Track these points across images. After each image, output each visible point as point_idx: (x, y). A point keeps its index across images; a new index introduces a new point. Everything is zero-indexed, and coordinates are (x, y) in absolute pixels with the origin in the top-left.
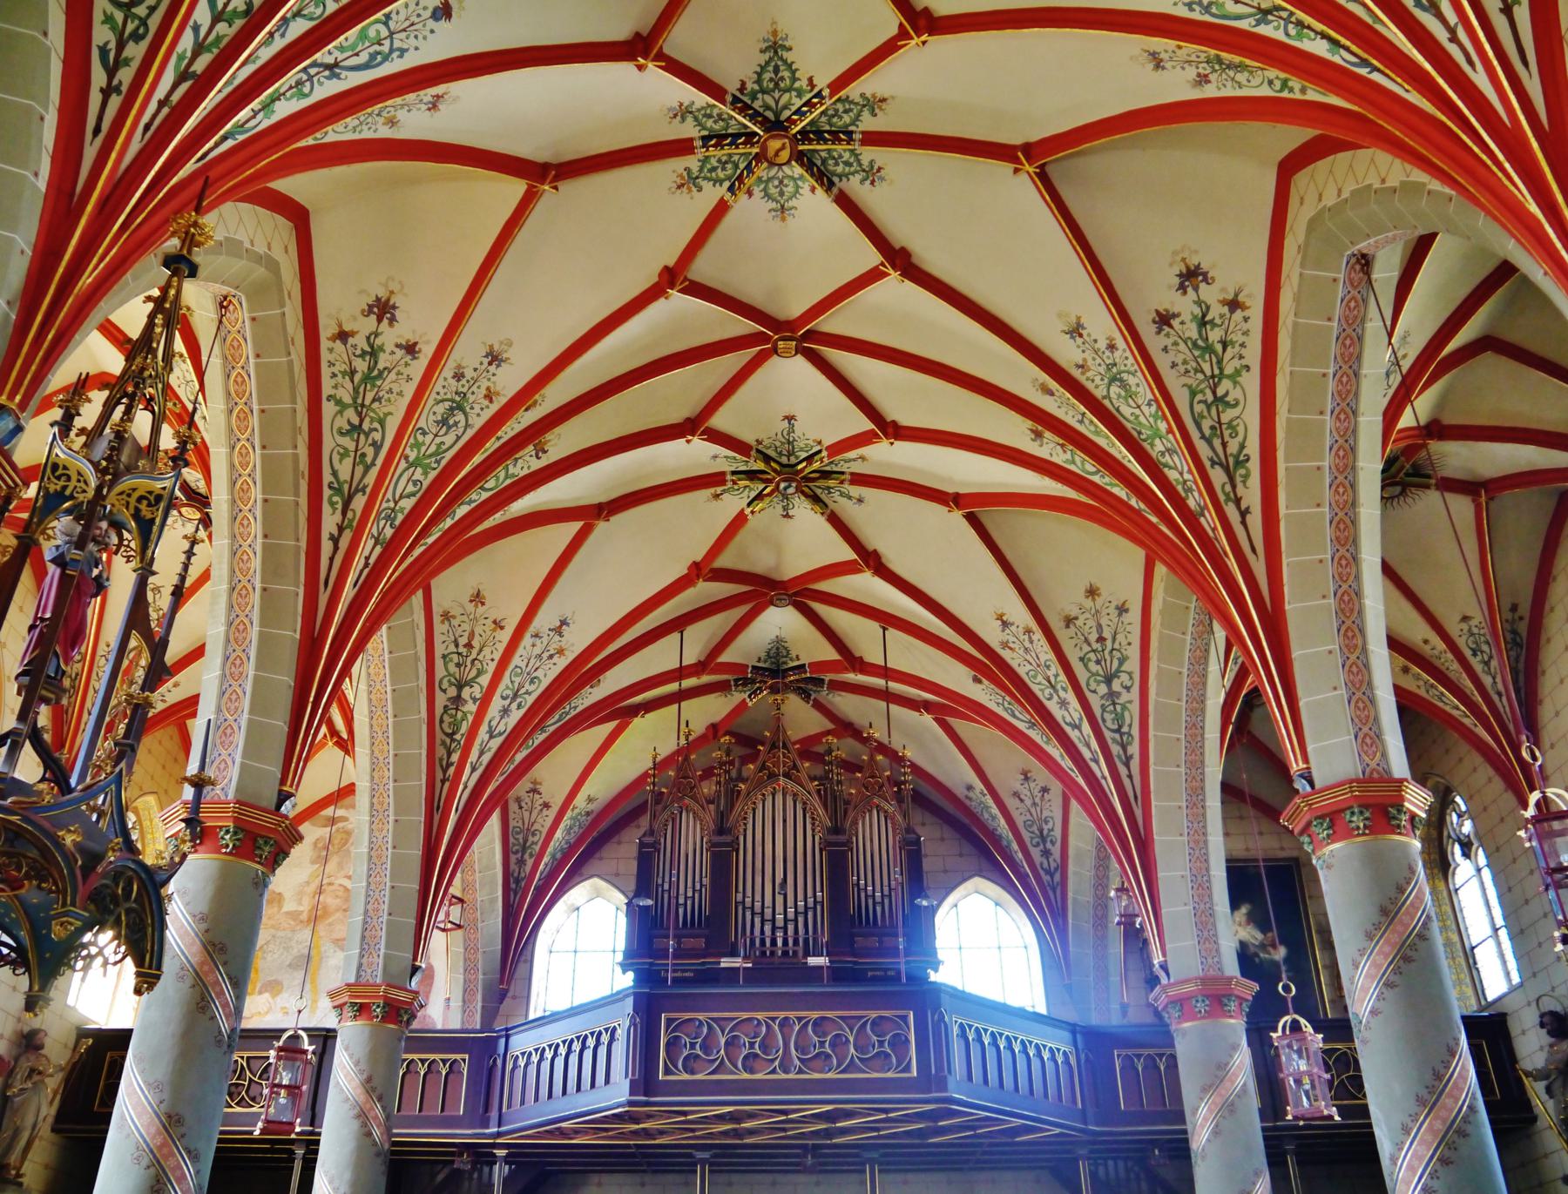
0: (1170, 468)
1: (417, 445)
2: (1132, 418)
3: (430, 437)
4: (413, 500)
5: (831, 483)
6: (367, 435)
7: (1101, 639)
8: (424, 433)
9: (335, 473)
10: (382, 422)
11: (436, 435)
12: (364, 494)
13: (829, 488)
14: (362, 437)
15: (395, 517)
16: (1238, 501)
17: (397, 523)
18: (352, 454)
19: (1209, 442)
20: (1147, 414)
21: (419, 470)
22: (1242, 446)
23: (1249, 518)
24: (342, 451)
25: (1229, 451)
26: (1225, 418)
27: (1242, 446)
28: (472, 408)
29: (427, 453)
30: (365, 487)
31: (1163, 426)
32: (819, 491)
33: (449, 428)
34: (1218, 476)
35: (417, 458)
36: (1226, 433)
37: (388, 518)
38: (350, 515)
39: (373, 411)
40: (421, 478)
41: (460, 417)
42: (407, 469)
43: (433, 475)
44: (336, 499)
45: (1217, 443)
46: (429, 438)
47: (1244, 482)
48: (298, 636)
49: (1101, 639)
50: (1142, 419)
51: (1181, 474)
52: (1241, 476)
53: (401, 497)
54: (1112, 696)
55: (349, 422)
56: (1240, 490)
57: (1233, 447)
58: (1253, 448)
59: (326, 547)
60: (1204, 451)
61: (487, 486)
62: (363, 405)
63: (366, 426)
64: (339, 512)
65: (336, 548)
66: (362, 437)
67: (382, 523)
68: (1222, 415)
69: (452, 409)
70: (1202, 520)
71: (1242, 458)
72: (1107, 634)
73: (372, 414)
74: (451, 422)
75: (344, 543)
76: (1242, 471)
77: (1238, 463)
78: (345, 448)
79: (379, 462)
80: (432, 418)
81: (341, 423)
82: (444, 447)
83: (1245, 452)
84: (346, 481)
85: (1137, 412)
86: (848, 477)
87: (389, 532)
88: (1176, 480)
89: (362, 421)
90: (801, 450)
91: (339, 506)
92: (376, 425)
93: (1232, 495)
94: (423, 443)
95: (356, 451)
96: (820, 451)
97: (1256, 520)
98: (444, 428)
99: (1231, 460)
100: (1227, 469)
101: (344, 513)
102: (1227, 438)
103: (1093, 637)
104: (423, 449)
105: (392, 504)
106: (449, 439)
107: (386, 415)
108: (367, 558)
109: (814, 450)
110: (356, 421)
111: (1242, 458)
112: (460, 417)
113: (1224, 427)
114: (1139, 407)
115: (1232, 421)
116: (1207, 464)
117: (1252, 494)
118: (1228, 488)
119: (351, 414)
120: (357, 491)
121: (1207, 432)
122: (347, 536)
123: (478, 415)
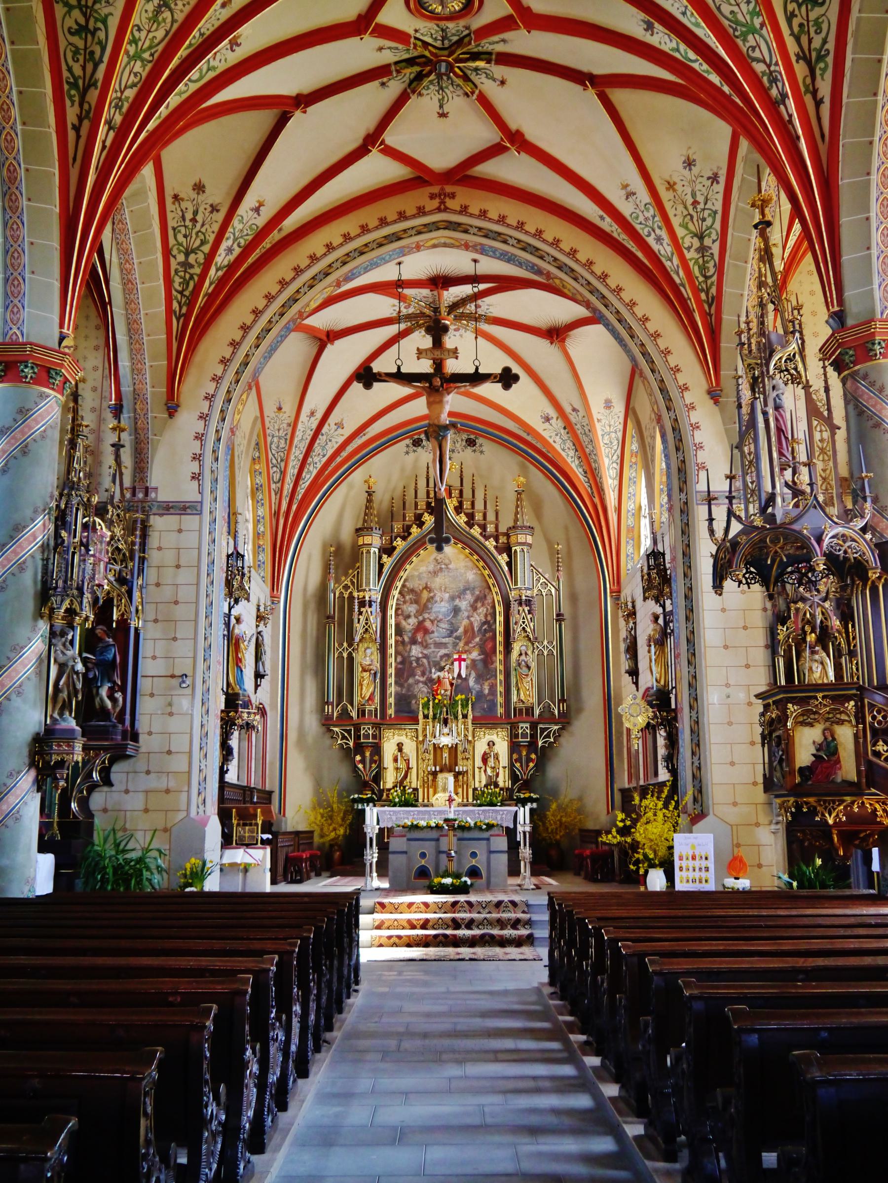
0: (758, 61)
1: (134, 41)
2: (730, 16)
3: (144, 34)
4: (135, 90)
5: (481, 64)
6: (93, 34)
7: (695, 203)
8: (139, 30)
9: (70, 69)
10: (104, 22)
11: (149, 31)
12: (96, 88)
13: (476, 69)
14: (89, 36)
15: (122, 104)
16: (814, 93)
17: (124, 110)
18: (82, 52)
19: (798, 39)
20: (745, 12)
21: (139, 63)
22: (825, 41)
23: (822, 106)
24: (73, 49)
25: (813, 46)
26: (813, 16)
27: (825, 41)
28: (176, 4)
29: (144, 47)
30: (96, 81)
31: (757, 22)
32: (469, 72)
33: (159, 24)
34: (801, 70)
35: (136, 52)
36: (812, 30)
37: (117, 107)
38: (86, 106)
39: (96, 11)
40: (140, 70)
41: (167, 14)
42: (129, 63)
43: (149, 66)
44: (73, 92)
45: (804, 40)
46: (144, 34)
47: (822, 75)
48: (57, 210)
49: (695, 203)
50: (740, 17)
51: (769, 66)
52: (820, 69)
53: (126, 87)
54: (702, 249)
55: (76, 21)
56: (819, 83)
57: (817, 43)
58: (831, 46)
59: (71, 134)
60: (792, 47)
61: (193, 78)
62: (87, 7)
63: (91, 25)
64: (77, 104)
65: (78, 137)
66: (89, 36)
67: (112, 110)
68: (810, 13)
69: (160, 6)
70: (782, 107)
71: (823, 53)
72: (701, 199)
73: (95, 15)
74: (160, 19)
75: (84, 131)
76: (822, 65)
77: (820, 58)
78: (76, 47)
79: (106, 59)
80: (144, 15)
81: (70, 23)
82: (156, 41)
83: (826, 47)
84: (79, 77)
85: (736, 9)
86: (494, 57)
87: (118, 119)
88: (764, 73)
89: (87, 21)
90: (454, 35)
91: (77, 99)
92: (100, 25)
93: (811, 87)
94: (140, 39)
95: (85, 49)
96: (469, 35)
97: (826, 109)
98: (155, 25)
99: (814, 54)
100: (809, 62)
101: (81, 105)
102: (812, 34)
103: (690, 200)
104: (140, 44)
105: (119, 94)
106: (160, 34)
107: (107, 16)
108: (104, 142)
109: (465, 33)
110: (82, 21)
111: (823, 53)
112: (167, 14)
113: (811, 24)
114: (738, 5)
115: (818, 18)
116: (793, 59)
117: (825, 88)
118: (808, 81)
119: (76, 13)
120: (89, 86)
121: (796, 29)
122: (86, 124)
123: (182, 11)
